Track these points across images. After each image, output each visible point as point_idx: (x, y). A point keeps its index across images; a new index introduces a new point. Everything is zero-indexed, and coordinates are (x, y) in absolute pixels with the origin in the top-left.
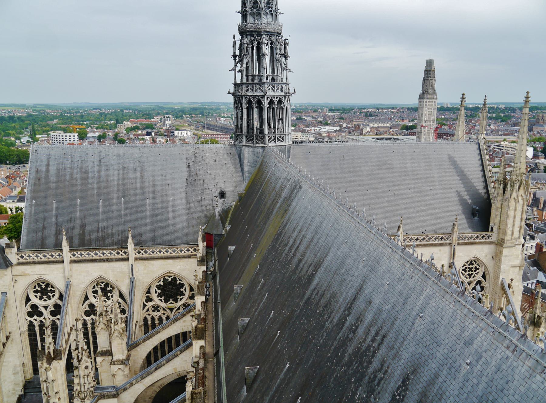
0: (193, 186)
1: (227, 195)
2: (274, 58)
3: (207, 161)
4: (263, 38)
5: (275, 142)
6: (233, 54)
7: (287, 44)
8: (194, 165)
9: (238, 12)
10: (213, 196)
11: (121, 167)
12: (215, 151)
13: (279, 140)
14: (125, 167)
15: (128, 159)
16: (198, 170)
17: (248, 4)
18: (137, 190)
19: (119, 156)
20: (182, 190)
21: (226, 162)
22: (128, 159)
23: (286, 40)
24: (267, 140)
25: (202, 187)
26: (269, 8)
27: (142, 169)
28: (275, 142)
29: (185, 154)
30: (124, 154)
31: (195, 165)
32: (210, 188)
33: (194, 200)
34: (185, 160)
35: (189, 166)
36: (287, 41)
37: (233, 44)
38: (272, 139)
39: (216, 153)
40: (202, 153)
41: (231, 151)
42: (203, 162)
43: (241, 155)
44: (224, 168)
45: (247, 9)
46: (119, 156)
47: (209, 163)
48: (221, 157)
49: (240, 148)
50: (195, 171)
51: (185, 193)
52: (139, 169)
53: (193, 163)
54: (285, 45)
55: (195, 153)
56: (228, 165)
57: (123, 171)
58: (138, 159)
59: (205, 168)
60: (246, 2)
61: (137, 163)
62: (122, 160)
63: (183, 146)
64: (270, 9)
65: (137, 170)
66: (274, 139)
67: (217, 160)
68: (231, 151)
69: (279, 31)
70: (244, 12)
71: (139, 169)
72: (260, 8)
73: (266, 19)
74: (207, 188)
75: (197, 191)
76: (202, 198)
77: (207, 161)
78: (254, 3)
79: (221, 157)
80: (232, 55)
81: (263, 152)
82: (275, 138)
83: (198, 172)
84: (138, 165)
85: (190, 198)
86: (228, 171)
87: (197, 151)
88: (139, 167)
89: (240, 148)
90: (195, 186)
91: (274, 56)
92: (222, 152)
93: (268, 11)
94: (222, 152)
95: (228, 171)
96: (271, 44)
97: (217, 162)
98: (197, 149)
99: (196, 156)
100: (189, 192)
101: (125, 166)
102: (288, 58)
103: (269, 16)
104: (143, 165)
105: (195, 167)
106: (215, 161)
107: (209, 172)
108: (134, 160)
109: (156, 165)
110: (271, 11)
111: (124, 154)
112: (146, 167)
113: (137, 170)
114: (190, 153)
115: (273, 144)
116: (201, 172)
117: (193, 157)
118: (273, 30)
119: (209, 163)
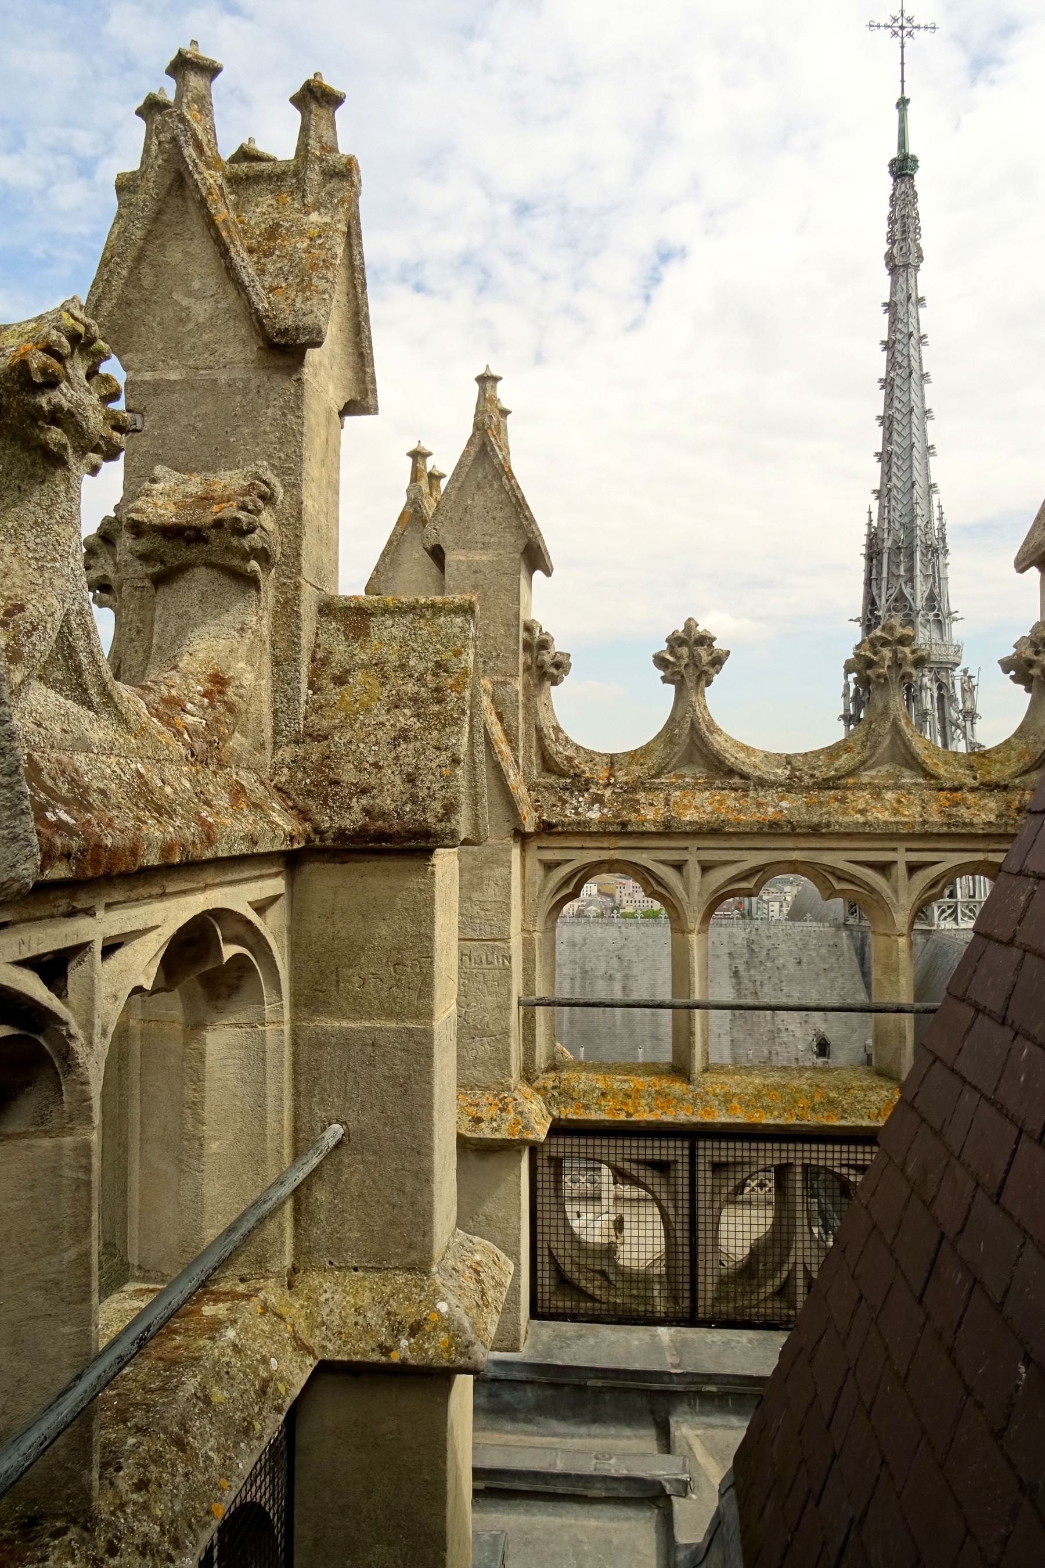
0: (749, 1021)
1: (833, 1048)
2: (947, 720)
3: (781, 961)
4: (923, 676)
5: (956, 919)
6: (842, 713)
7: (974, 687)
8: (748, 970)
9: (856, 621)
10: (798, 1050)
11: (578, 970)
12: (798, 938)
13: (964, 914)
14: (587, 972)
15: (594, 951)
16: (758, 983)
17: (882, 603)
18: (615, 1026)
19: (574, 945)
20: (722, 1031)
21: (826, 966)
22: (594, 951)
23: (970, 677)
24: (936, 914)
25: (770, 1027)
26: (935, 607)
27: (626, 977)
28: (956, 919)
29: (725, 943)
30: (585, 939)
31: (752, 972)
32: (791, 1028)
33: (751, 1056)
34: (726, 958)
35: (736, 973)
36: (974, 681)
37: (842, 690)
38: (949, 912)
39: (800, 944)
40: (767, 943)
41: (836, 940)
42: (769, 964)
43: (867, 949)
44: (823, 981)
45: (880, 613)
46: (574, 945)
47: (784, 966)
48: (814, 954)
49: (863, 932)
50: (750, 985)
51: (728, 1038)
52: (618, 976)
53: (745, 966)
54: (969, 690)
55: (750, 943)
56: (832, 974)
57: (583, 979)
58: (616, 953)
59: (775, 980)
60: (876, 598)
61: (615, 962)
62: (579, 955)
63: (721, 926)
64: (936, 612)
65: (614, 979)
66: (950, 915)
67: (805, 960)
68: (836, 940)
69: (956, 659)
70: (869, 620)
71: (618, 976)
72: (911, 609)
73: (928, 634)
74: (782, 1028)
75: (757, 1035)
76: (770, 1053)
77: (781, 961)
78: (896, 600)
79: (814, 954)
80: (841, 716)
81: (925, 944)
82: (955, 911)
83: (759, 989)
84: (616, 967)
85: (741, 1051)
86: (832, 988)
87: (753, 937)
88: (618, 971)
89: (863, 932)
90: (753, 1022)
91: (947, 715)
92: (814, 942)
93: (931, 617)
94: (814, 942)
95: (832, 988)
96: (940, 688)
97: (804, 966)
98: (754, 932)
99: (753, 950)
100: (740, 1036)
101: (587, 968)
102: (977, 720)
103: (933, 627)
104: (629, 967)
105: (750, 976)
106: (799, 963)
107: (786, 989)
108: (607, 956)
109: (659, 969)
110: (937, 615)
111: (585, 939)
112: (635, 972)
113: (614, 979)
114: (738, 941)
115: (948, 925)
116: (766, 989)
117: (745, 950)
118: (944, 659)
119: (784, 966)
